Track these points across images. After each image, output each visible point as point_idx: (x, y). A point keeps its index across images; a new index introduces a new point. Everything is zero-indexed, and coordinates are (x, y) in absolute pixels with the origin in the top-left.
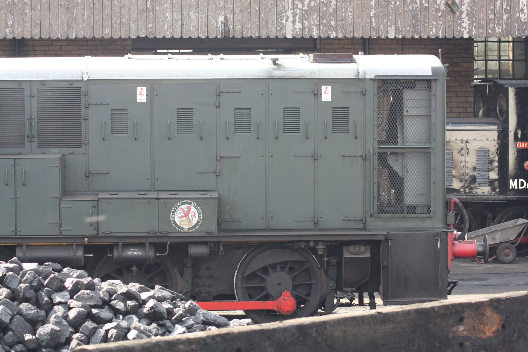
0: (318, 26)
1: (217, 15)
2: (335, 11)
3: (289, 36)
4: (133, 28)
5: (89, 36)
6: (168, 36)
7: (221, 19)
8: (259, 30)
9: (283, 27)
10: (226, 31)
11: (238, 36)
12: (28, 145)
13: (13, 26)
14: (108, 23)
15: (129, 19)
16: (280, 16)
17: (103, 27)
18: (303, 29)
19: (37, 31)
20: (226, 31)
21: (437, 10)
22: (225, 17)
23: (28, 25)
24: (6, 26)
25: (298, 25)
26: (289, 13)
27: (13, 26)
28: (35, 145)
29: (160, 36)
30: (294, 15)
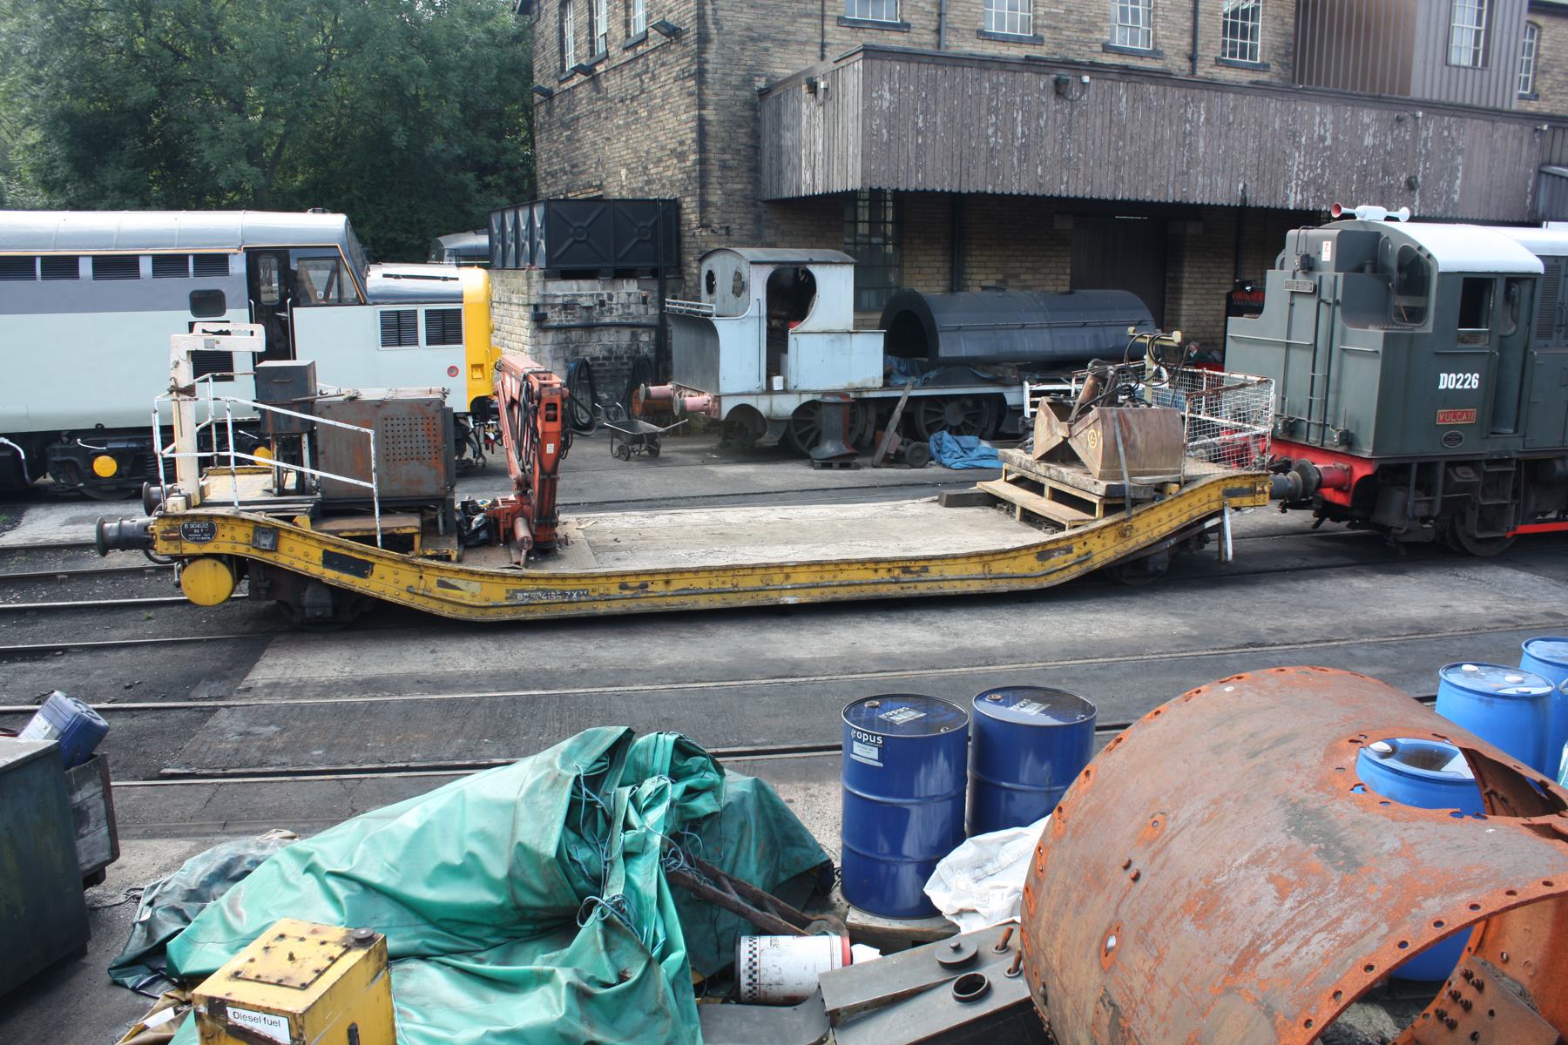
0: (1314, 198)
1: (1239, 182)
2: (1328, 183)
3: (1291, 208)
4: (1171, 191)
5: (1133, 198)
6: (1199, 202)
7: (1241, 186)
8: (1270, 200)
9: (1287, 198)
10: (1244, 199)
11: (1253, 205)
12: (1555, 334)
13: (1067, 182)
14: (1149, 185)
15: (1168, 182)
16: (1286, 187)
17: (1146, 188)
18: (1302, 201)
19: (1088, 189)
20: (1244, 199)
21: (1399, 188)
22: (1245, 185)
23: (1081, 182)
24: (1062, 183)
25: (1299, 197)
26: (1293, 184)
27: (1067, 182)
28: (1562, 334)
29: (1192, 202)
30: (1297, 185)
